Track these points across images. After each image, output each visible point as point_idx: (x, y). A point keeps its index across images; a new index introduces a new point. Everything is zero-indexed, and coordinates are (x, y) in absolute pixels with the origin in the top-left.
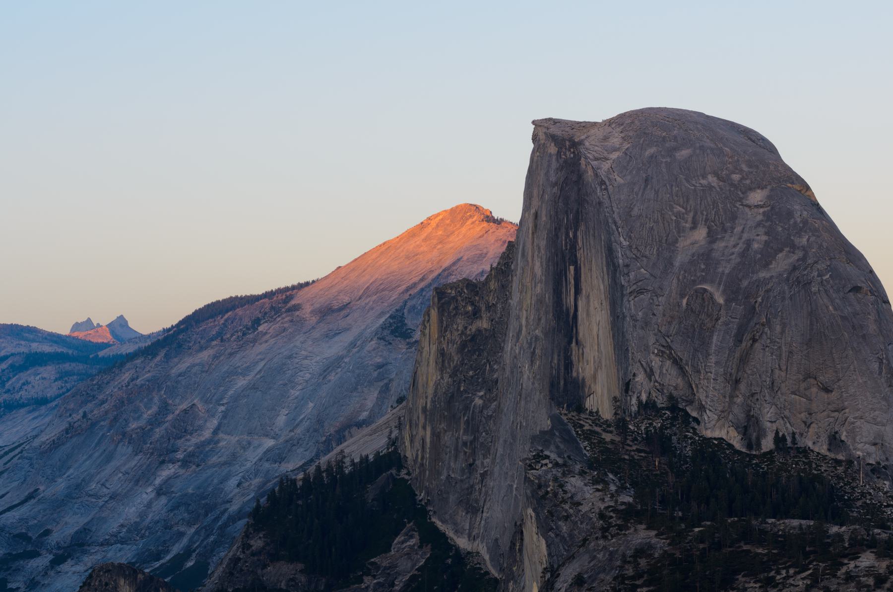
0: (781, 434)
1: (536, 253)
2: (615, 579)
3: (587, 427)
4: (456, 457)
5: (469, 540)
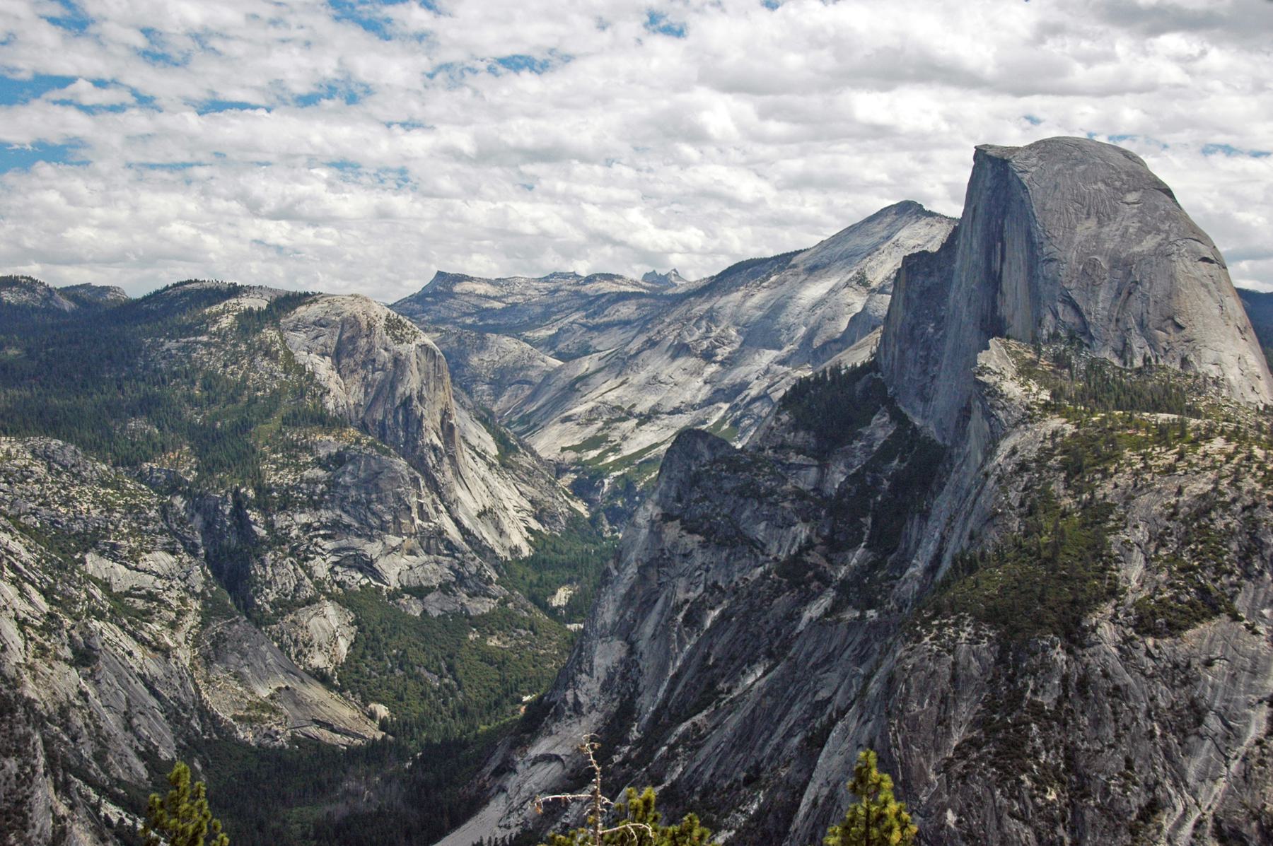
3: (1013, 349)
4: (915, 365)
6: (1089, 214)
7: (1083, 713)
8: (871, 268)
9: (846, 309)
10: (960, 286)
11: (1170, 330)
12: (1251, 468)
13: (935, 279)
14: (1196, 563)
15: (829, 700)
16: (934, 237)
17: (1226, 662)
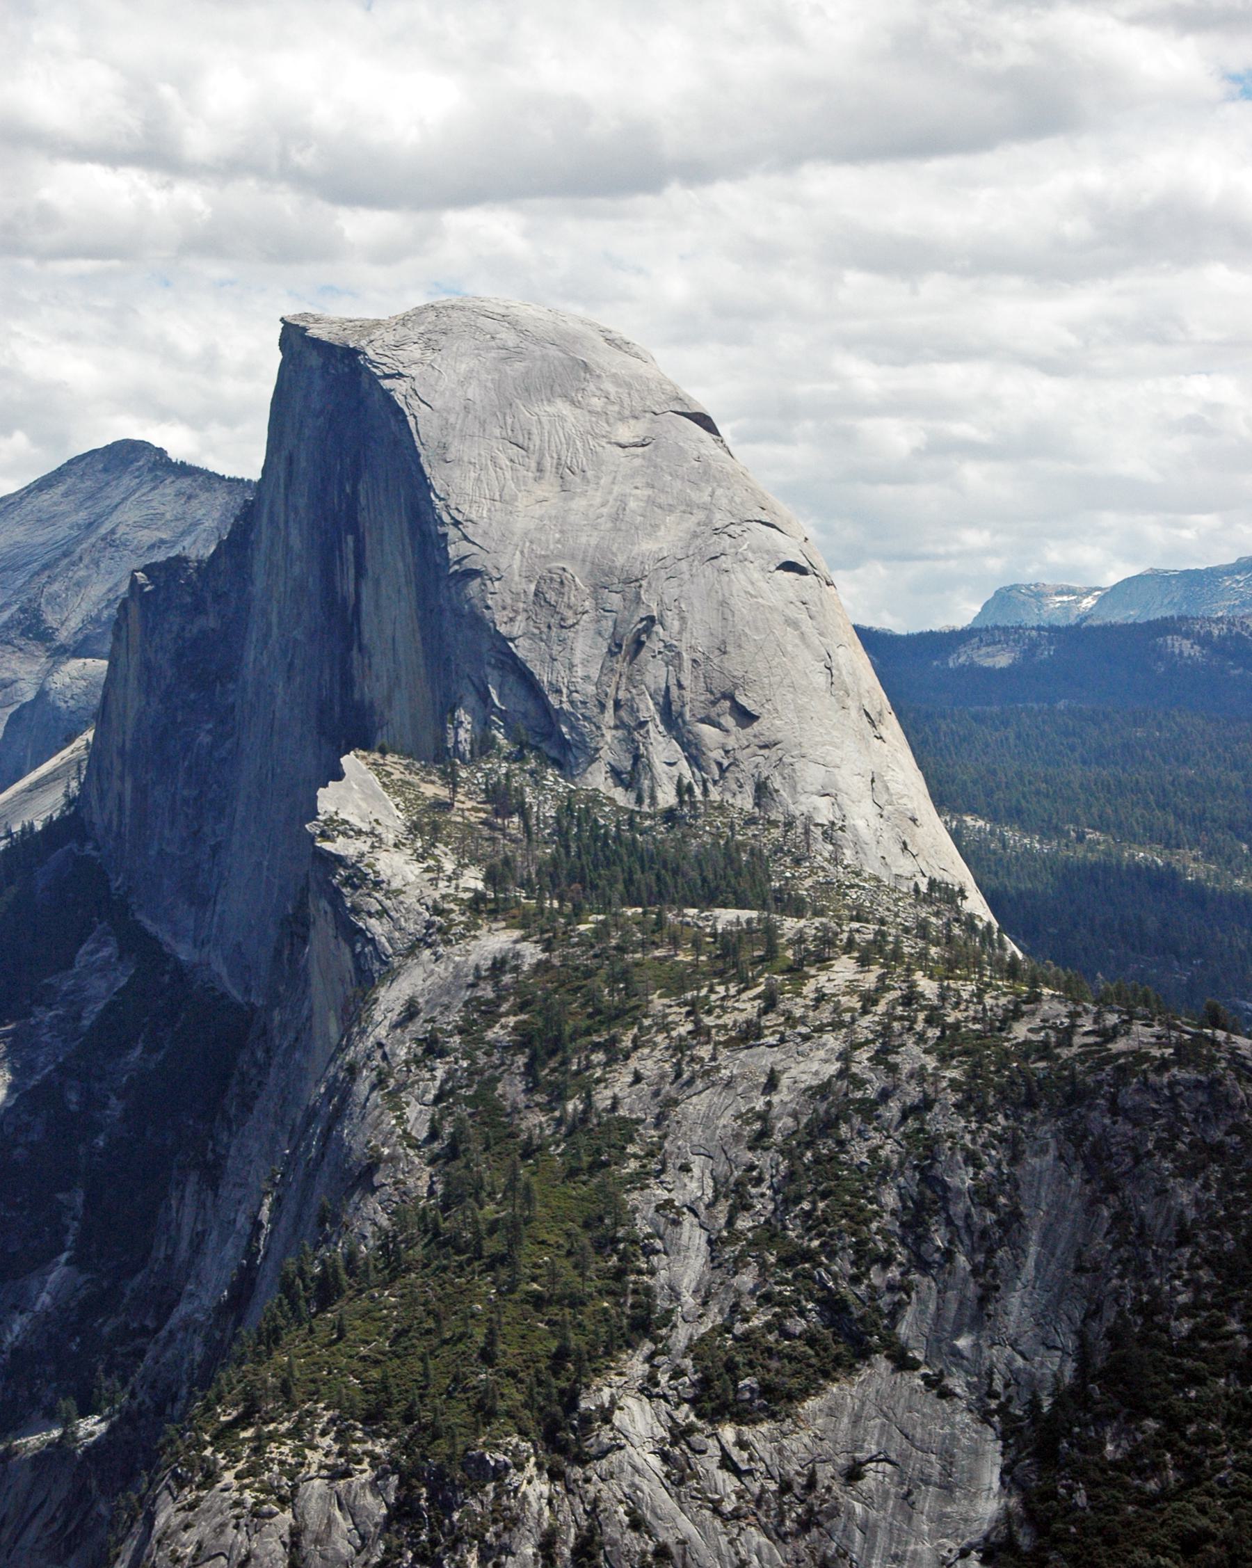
0: (686, 781)
1: (292, 515)
2: (466, 1004)
5: (195, 946)
6: (540, 469)
8: (53, 598)
10: (267, 635)
11: (729, 721)
12: (913, 1021)
13: (211, 622)
14: (816, 1243)
16: (197, 523)
17: (889, 1467)
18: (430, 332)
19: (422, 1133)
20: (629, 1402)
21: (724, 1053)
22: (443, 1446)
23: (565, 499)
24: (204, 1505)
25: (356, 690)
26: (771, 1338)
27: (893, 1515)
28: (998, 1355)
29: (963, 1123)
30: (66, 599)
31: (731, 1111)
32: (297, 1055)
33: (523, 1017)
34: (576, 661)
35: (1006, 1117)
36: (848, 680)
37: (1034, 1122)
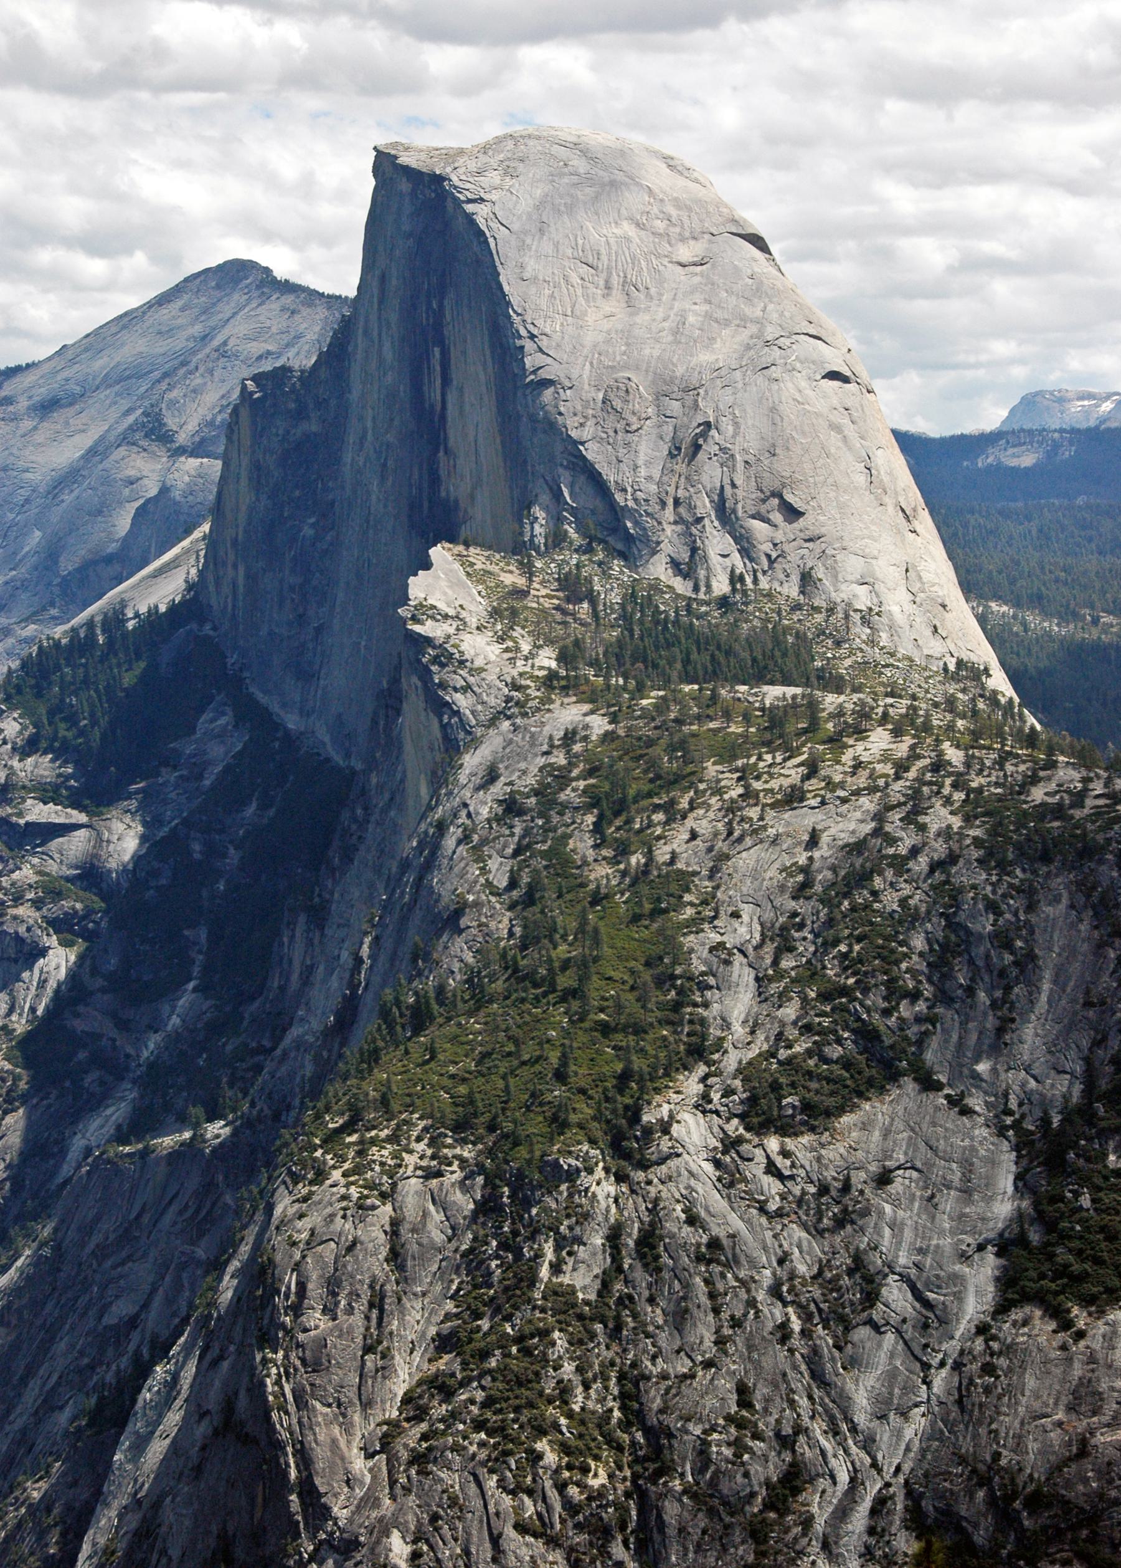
0: (738, 572)
1: (384, 329)
2: (541, 769)
3: (479, 566)
6: (608, 287)
7: (651, 1300)
8: (173, 403)
9: (126, 492)
10: (363, 438)
11: (777, 517)
12: (941, 786)
13: (314, 428)
14: (851, 981)
15: (132, 1322)
16: (298, 337)
17: (915, 1174)
18: (509, 159)
19: (502, 882)
20: (686, 1116)
21: (771, 814)
22: (523, 1152)
23: (631, 315)
24: (315, 1198)
25: (443, 488)
26: (811, 1062)
27: (918, 1215)
28: (1014, 1079)
29: (984, 876)
30: (184, 404)
31: (777, 865)
32: (392, 813)
33: (592, 781)
34: (640, 462)
35: (1024, 870)
36: (886, 479)
37: (1048, 875)
